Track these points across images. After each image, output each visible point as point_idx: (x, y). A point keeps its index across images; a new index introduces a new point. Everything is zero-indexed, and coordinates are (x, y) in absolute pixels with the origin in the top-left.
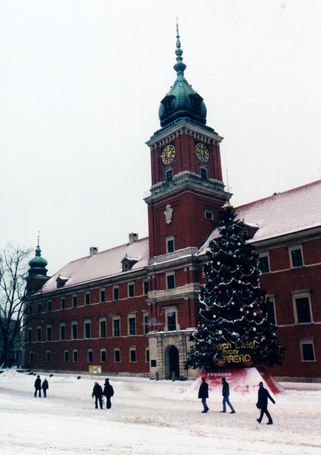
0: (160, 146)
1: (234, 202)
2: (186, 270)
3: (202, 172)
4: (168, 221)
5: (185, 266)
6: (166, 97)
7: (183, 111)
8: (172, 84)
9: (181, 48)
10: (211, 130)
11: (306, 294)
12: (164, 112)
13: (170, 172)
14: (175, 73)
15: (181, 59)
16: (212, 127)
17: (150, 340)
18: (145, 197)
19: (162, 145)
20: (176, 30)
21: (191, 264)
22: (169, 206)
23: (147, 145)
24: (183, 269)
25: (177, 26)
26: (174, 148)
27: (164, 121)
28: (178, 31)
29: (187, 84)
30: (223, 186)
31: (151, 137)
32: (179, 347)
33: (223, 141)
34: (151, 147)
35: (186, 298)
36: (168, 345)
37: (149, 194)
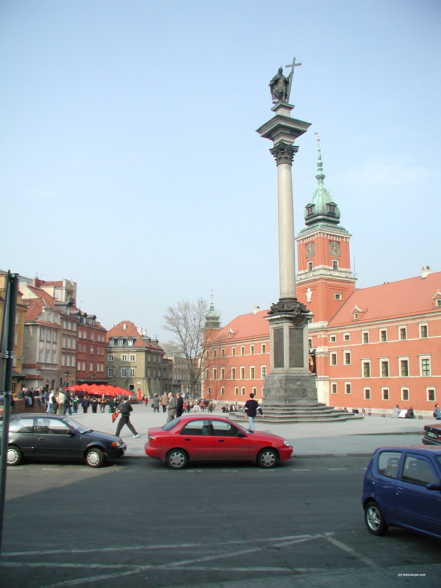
1: (357, 286)
2: (319, 337)
3: (334, 264)
4: (309, 301)
9: (322, 161)
10: (343, 229)
15: (322, 169)
16: (344, 227)
21: (322, 333)
22: (309, 290)
27: (307, 222)
30: (350, 273)
35: (318, 356)
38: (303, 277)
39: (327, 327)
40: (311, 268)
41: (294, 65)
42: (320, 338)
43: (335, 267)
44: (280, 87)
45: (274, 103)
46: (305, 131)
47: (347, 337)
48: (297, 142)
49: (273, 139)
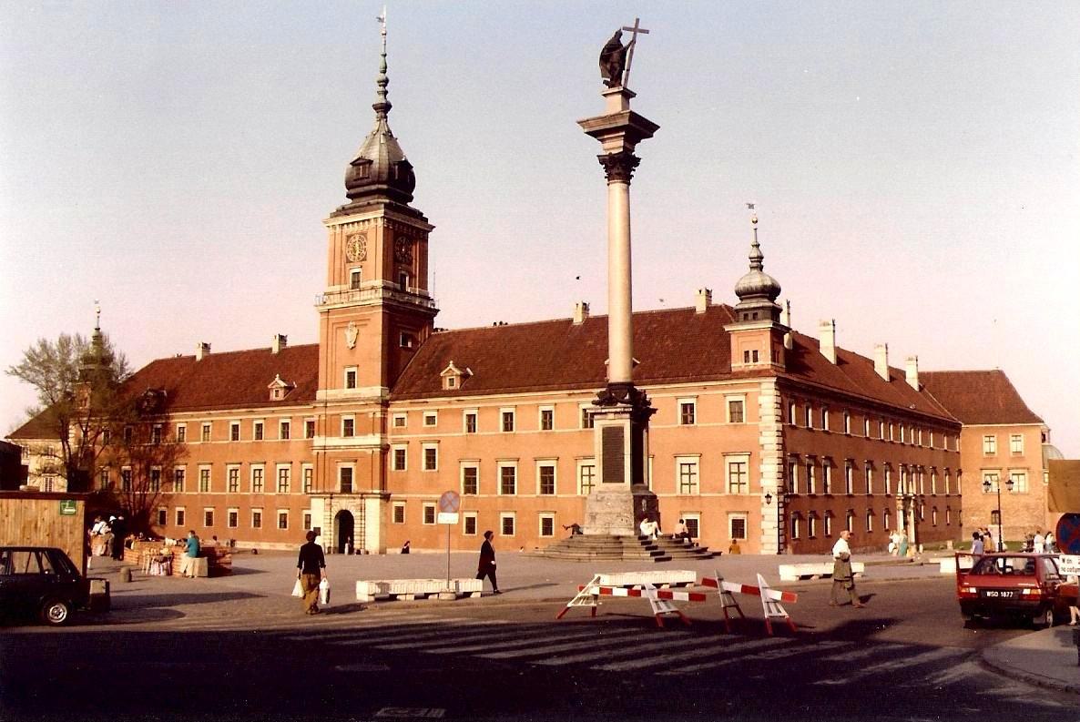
1: (438, 322)
5: (372, 410)
6: (359, 159)
7: (385, 187)
10: (418, 215)
11: (512, 462)
12: (355, 180)
15: (386, 93)
17: (313, 501)
24: (367, 413)
27: (353, 191)
29: (391, 136)
30: (428, 299)
32: (355, 514)
33: (434, 230)
36: (340, 509)
38: (336, 298)
39: (388, 397)
40: (356, 284)
41: (635, 30)
42: (373, 418)
43: (403, 284)
44: (614, 60)
45: (605, 82)
46: (652, 136)
47: (430, 420)
48: (640, 149)
49: (602, 141)
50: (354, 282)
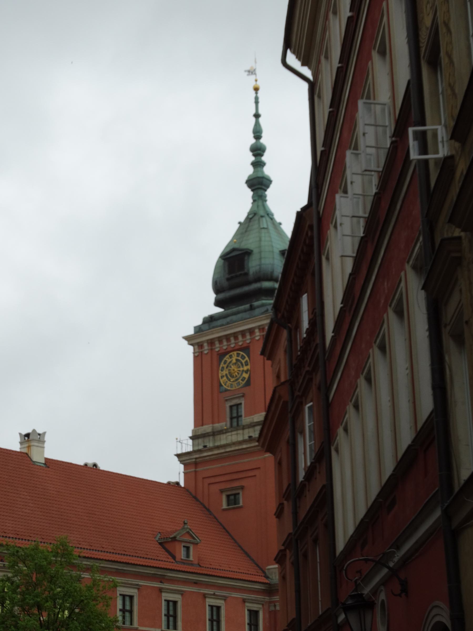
0: (217, 350)
6: (234, 250)
8: (242, 219)
12: (228, 279)
13: (238, 405)
14: (249, 193)
18: (179, 452)
19: (221, 348)
20: (253, 100)
23: (186, 342)
25: (256, 89)
26: (247, 358)
28: (257, 102)
31: (195, 328)
34: (196, 347)
37: (188, 446)
50: (232, 418)
